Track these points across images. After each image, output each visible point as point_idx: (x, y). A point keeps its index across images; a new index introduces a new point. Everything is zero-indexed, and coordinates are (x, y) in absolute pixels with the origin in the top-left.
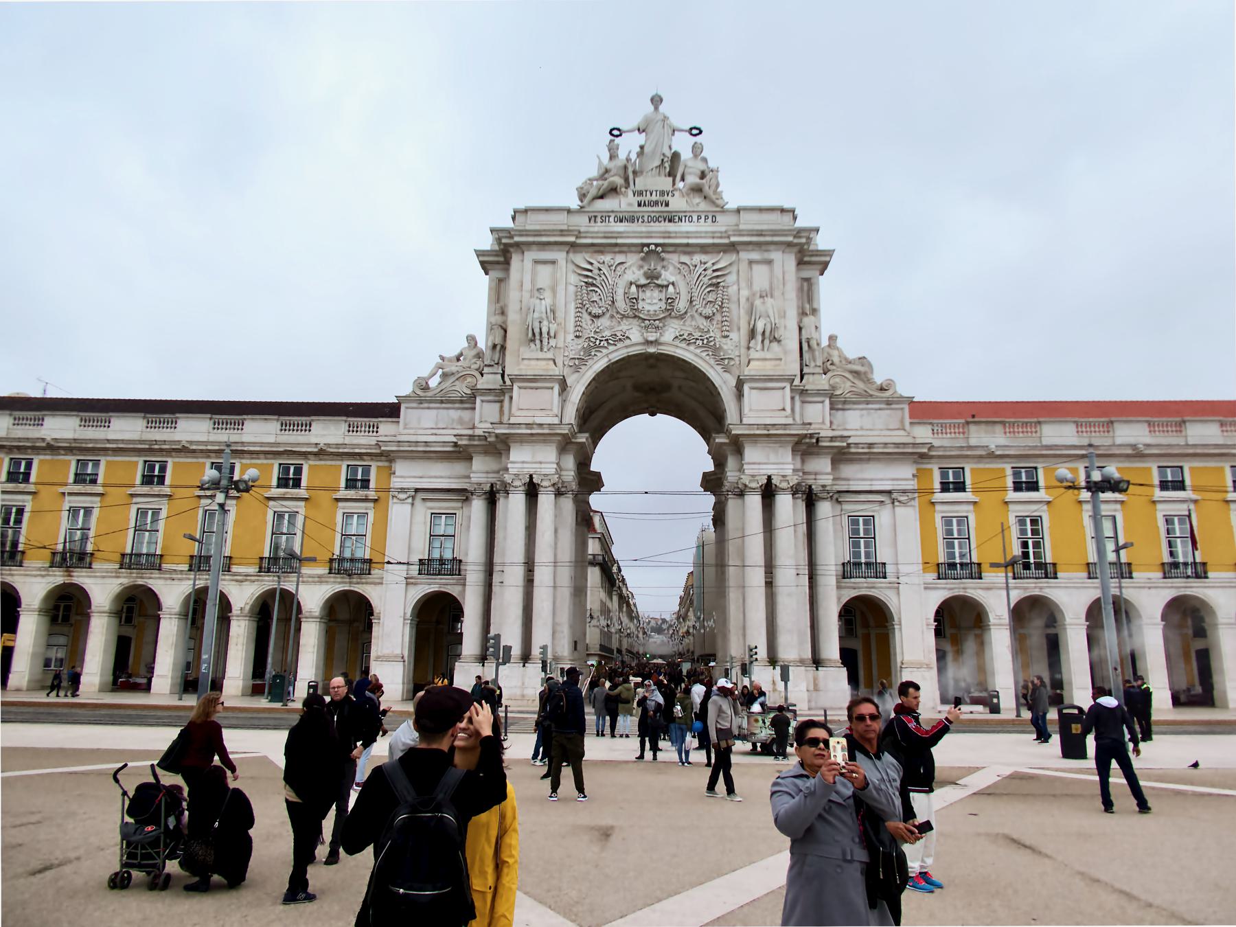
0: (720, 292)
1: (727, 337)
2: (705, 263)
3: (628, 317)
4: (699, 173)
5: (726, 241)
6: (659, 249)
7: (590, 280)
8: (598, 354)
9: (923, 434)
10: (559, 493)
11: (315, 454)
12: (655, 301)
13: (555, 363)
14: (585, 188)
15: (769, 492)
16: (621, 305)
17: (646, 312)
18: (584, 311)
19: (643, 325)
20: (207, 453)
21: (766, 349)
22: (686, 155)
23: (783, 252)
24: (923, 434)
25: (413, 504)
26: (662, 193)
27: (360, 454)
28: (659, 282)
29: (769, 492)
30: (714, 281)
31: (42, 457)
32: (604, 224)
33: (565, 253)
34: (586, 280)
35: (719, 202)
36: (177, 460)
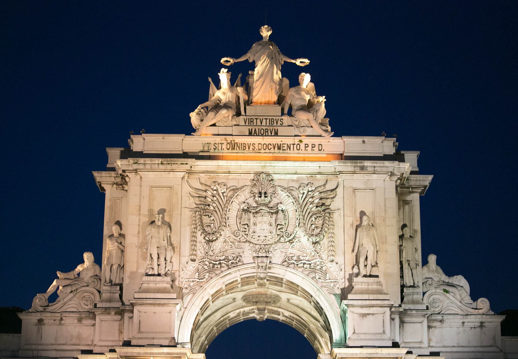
1: (332, 261)
3: (239, 242)
23: (384, 180)
26: (271, 121)
32: (216, 151)
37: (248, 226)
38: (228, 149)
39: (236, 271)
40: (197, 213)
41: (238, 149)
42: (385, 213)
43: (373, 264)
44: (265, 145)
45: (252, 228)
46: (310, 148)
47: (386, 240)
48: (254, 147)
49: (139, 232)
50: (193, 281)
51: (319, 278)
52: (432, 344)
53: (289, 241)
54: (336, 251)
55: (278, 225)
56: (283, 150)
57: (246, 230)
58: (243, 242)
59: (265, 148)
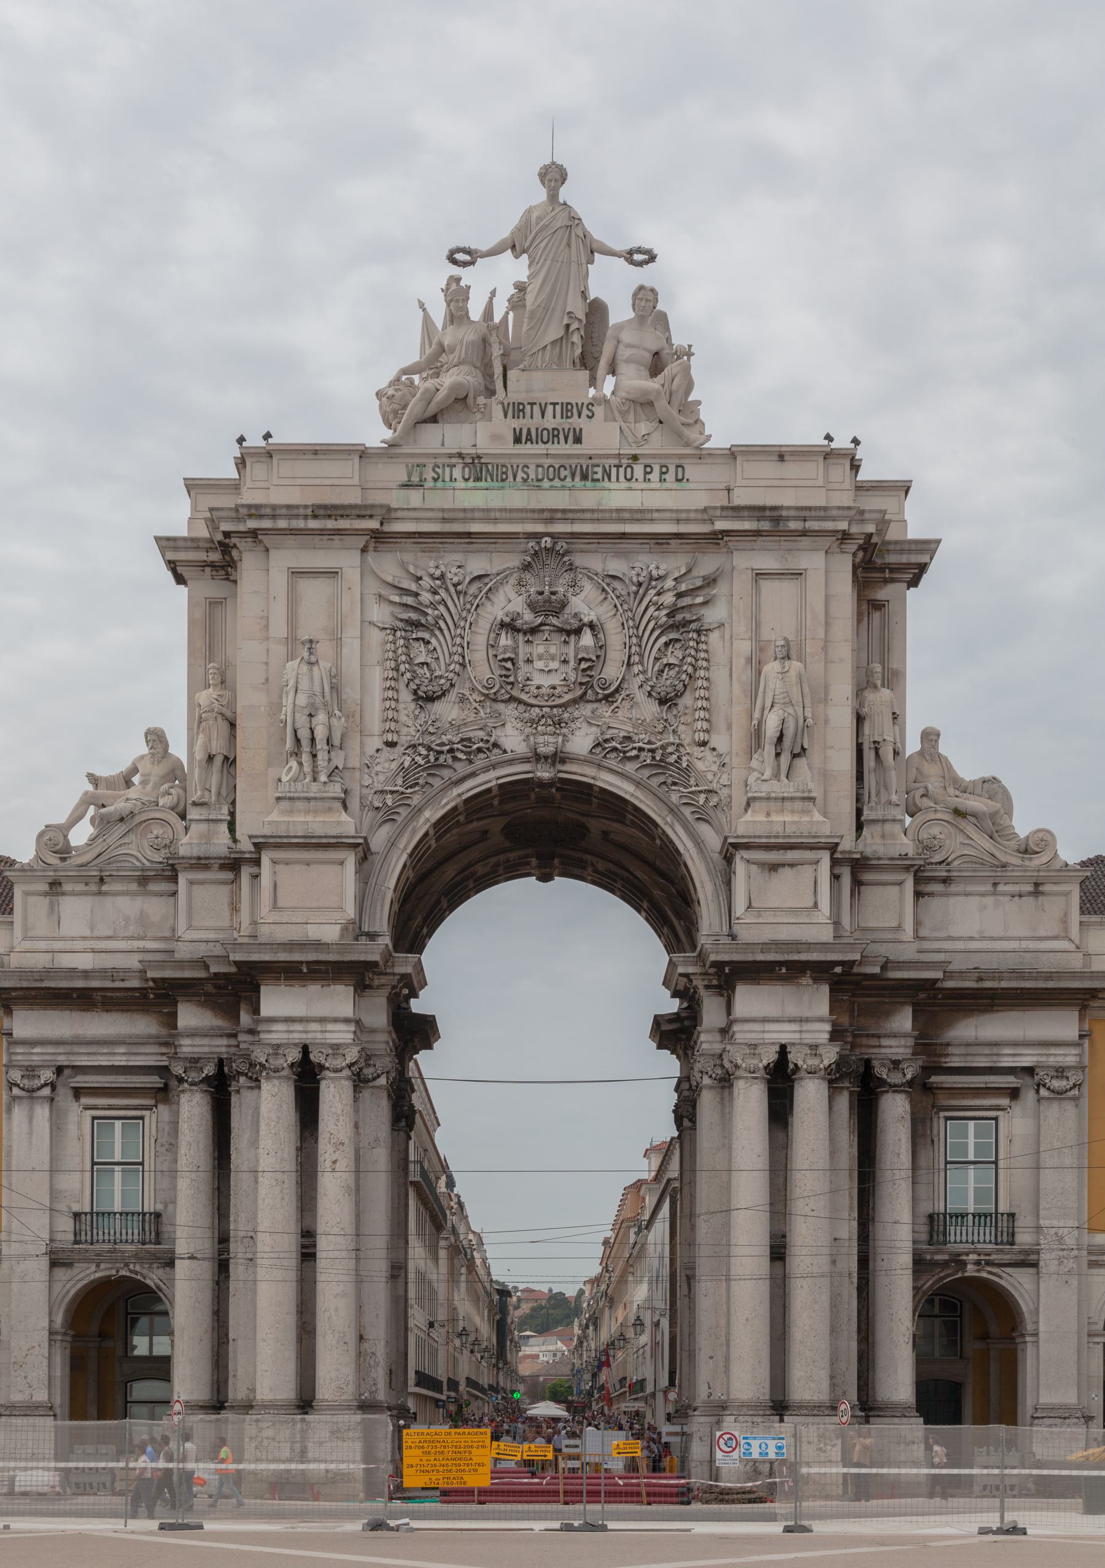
0: (692, 643)
1: (704, 744)
2: (660, 578)
3: (495, 700)
4: (648, 357)
7: (414, 616)
8: (437, 783)
10: (360, 1081)
13: (345, 808)
14: (400, 393)
16: (482, 670)
17: (533, 689)
18: (402, 686)
19: (527, 715)
21: (783, 777)
22: (620, 312)
23: (826, 552)
25: (52, 1099)
26: (567, 409)
30: (679, 617)
32: (439, 484)
33: (356, 556)
34: (405, 616)
35: (692, 434)
37: (514, 664)
38: (467, 480)
39: (486, 770)
40: (398, 634)
41: (489, 479)
42: (826, 632)
43: (795, 752)
44: (551, 469)
45: (524, 670)
46: (655, 476)
47: (826, 694)
48: (526, 473)
49: (267, 679)
50: (392, 792)
51: (674, 784)
52: (923, 933)
53: (606, 698)
54: (714, 719)
55: (581, 660)
56: (593, 480)
57: (508, 673)
58: (502, 701)
59: (551, 477)
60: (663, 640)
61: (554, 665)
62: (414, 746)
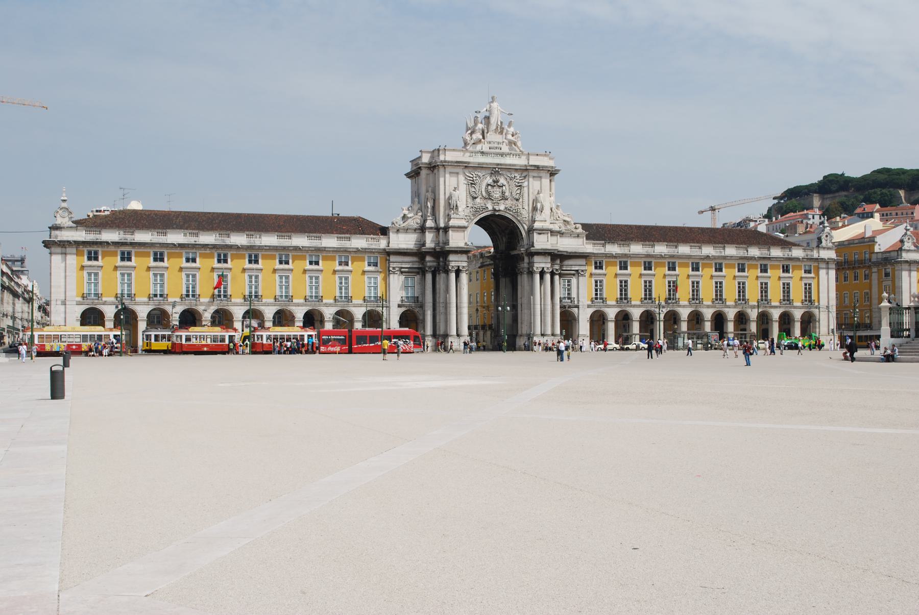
5: (525, 168)
6: (499, 170)
7: (473, 182)
9: (589, 247)
11: (354, 252)
12: (498, 193)
15: (542, 274)
20: (307, 251)
24: (589, 247)
26: (498, 143)
27: (374, 252)
28: (498, 184)
29: (542, 274)
31: (232, 252)
34: (471, 182)
36: (293, 254)
39: (485, 212)
60: (517, 188)
61: (498, 193)
62: (472, 207)
